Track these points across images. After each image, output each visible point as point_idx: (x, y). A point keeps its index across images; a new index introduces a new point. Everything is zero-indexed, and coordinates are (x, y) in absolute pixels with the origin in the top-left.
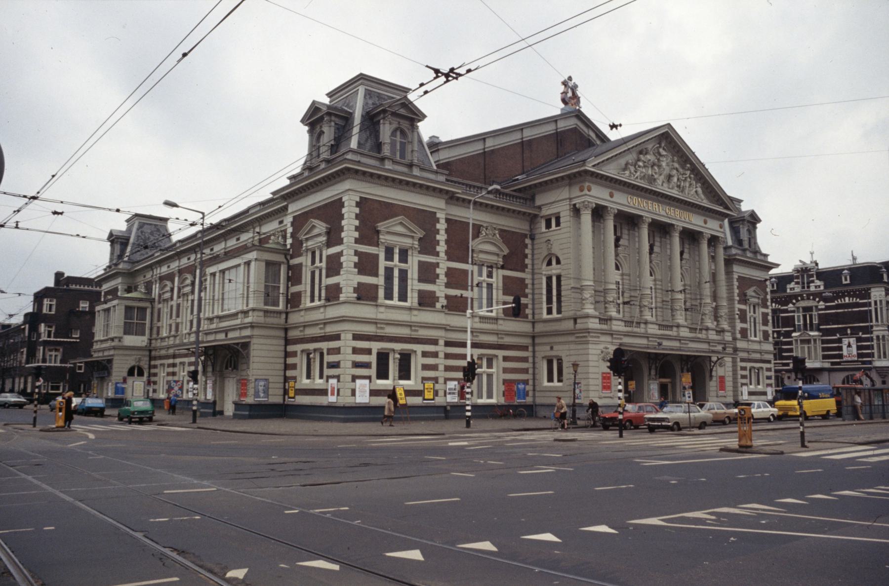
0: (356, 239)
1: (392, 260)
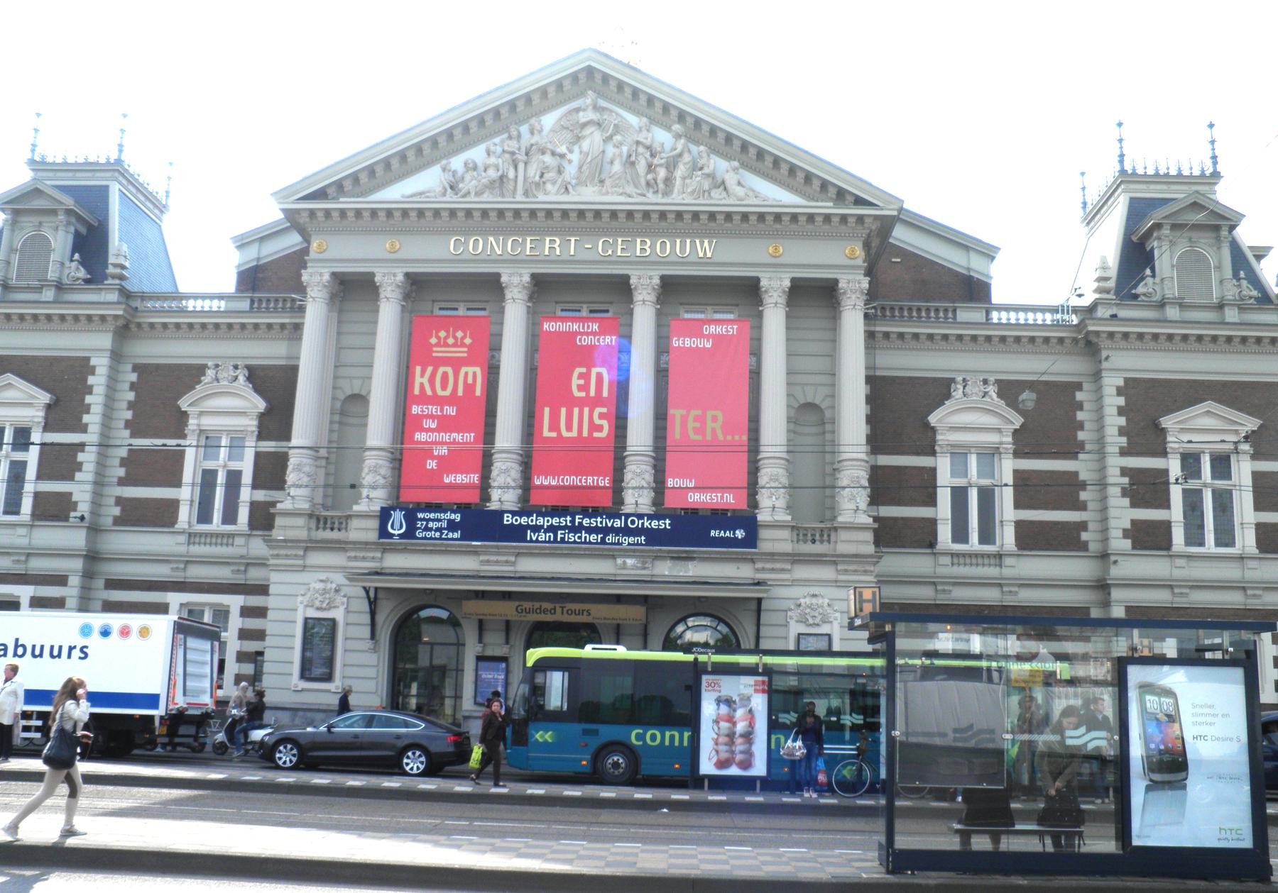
0: (1121, 448)
1: (1197, 474)
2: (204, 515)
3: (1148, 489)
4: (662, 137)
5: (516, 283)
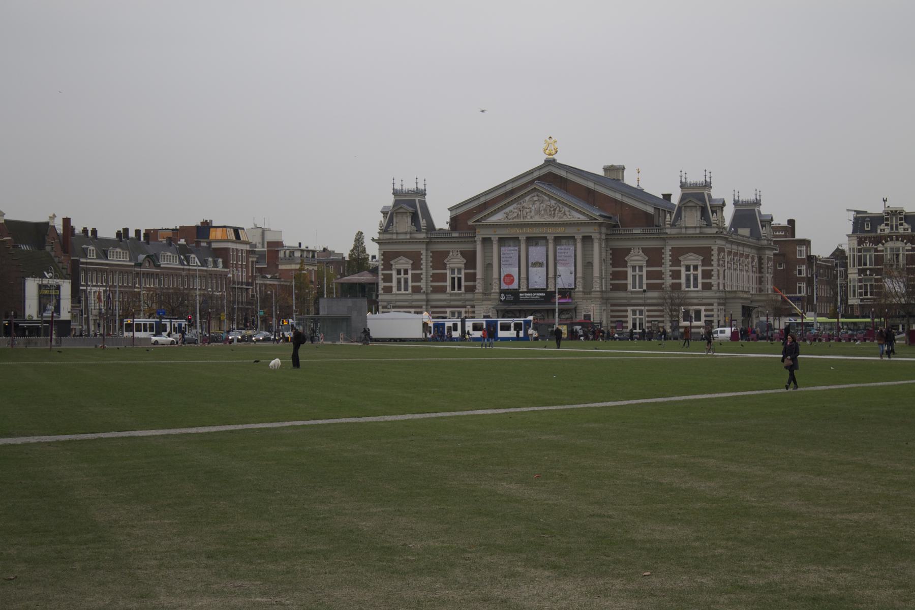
2: (453, 289)
3: (676, 275)
4: (553, 202)
5: (523, 238)
